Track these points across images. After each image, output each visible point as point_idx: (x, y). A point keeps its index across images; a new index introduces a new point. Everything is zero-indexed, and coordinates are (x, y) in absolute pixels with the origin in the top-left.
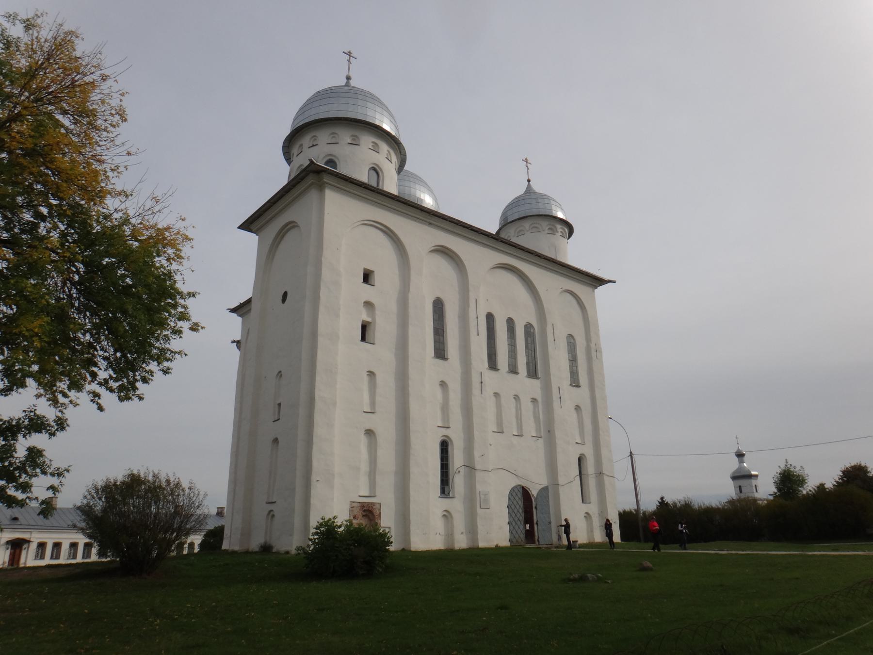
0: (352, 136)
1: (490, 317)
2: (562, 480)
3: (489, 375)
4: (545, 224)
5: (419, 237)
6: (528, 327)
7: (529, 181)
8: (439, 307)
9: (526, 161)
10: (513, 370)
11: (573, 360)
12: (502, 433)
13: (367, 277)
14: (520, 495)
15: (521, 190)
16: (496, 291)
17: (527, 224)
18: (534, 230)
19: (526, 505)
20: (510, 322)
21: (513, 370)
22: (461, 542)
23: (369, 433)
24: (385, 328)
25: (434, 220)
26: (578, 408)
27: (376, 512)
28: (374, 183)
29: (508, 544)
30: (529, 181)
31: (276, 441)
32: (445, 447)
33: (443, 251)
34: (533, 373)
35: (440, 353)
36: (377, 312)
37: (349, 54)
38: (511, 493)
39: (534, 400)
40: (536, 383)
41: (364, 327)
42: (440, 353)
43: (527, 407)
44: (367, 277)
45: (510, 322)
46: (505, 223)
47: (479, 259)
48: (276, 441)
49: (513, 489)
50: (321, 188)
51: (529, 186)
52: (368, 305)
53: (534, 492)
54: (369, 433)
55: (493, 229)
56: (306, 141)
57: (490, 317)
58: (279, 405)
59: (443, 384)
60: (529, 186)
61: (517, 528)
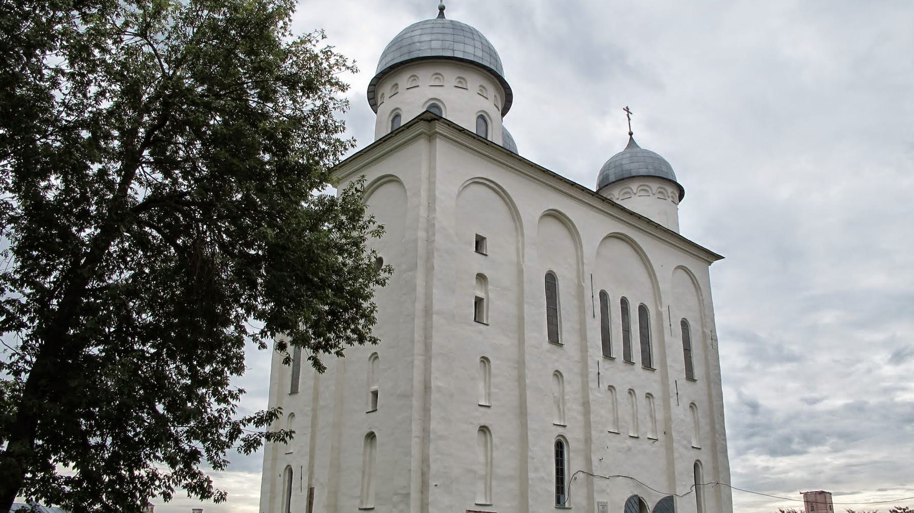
1: (603, 295)
2: (680, 491)
3: (605, 365)
4: (655, 186)
5: (533, 201)
6: (643, 310)
7: (631, 134)
8: (551, 280)
9: (627, 109)
10: (628, 359)
11: (687, 350)
13: (480, 243)
14: (637, 507)
15: (620, 146)
16: (597, 260)
17: (634, 186)
18: (643, 193)
20: (624, 302)
21: (628, 359)
23: (484, 429)
24: (499, 305)
26: (693, 405)
28: (483, 136)
30: (631, 134)
31: (371, 436)
32: (560, 447)
33: (554, 215)
34: (647, 364)
35: (554, 337)
36: (490, 287)
39: (649, 396)
41: (478, 302)
42: (554, 337)
44: (480, 243)
45: (624, 302)
46: (606, 183)
47: (593, 225)
48: (371, 436)
49: (629, 500)
50: (431, 137)
51: (631, 138)
52: (481, 277)
53: (651, 505)
56: (404, 80)
57: (603, 295)
58: (375, 394)
59: (558, 374)
60: (631, 138)
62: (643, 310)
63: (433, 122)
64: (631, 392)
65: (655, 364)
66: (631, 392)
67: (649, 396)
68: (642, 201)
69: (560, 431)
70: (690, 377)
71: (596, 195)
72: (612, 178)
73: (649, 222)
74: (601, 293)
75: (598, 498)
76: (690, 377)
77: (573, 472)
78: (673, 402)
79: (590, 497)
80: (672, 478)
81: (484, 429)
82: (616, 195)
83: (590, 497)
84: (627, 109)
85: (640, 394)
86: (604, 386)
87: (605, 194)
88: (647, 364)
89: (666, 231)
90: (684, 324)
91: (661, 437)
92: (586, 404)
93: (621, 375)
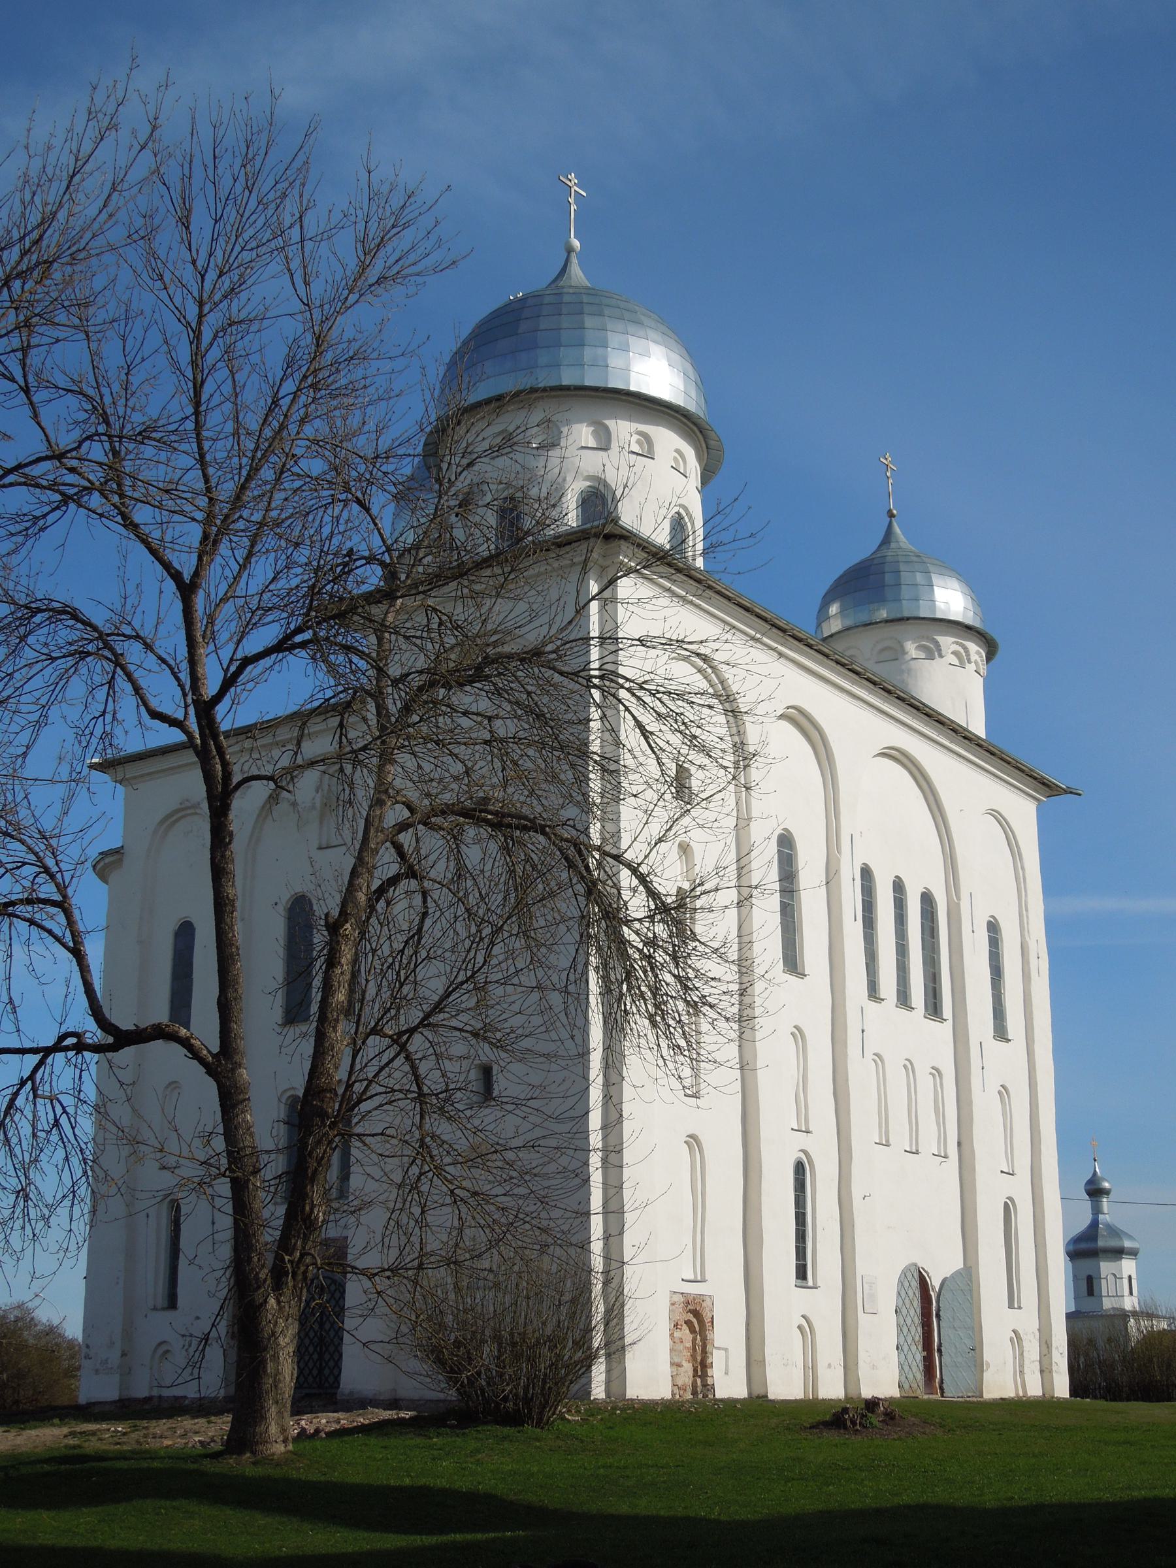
0: (678, 451)
1: (866, 873)
6: (927, 899)
10: (904, 999)
12: (917, 1153)
14: (915, 1284)
19: (932, 1310)
20: (899, 887)
21: (904, 999)
22: (832, 1389)
29: (895, 1393)
32: (800, 1168)
38: (901, 1283)
40: (943, 1031)
43: (925, 1083)
45: (899, 887)
49: (904, 1274)
53: (935, 1282)
54: (693, 1141)
57: (866, 873)
61: (910, 1357)
62: (927, 899)
63: (616, 543)
69: (802, 1141)
70: (1001, 1033)
74: (862, 869)
90: (993, 928)
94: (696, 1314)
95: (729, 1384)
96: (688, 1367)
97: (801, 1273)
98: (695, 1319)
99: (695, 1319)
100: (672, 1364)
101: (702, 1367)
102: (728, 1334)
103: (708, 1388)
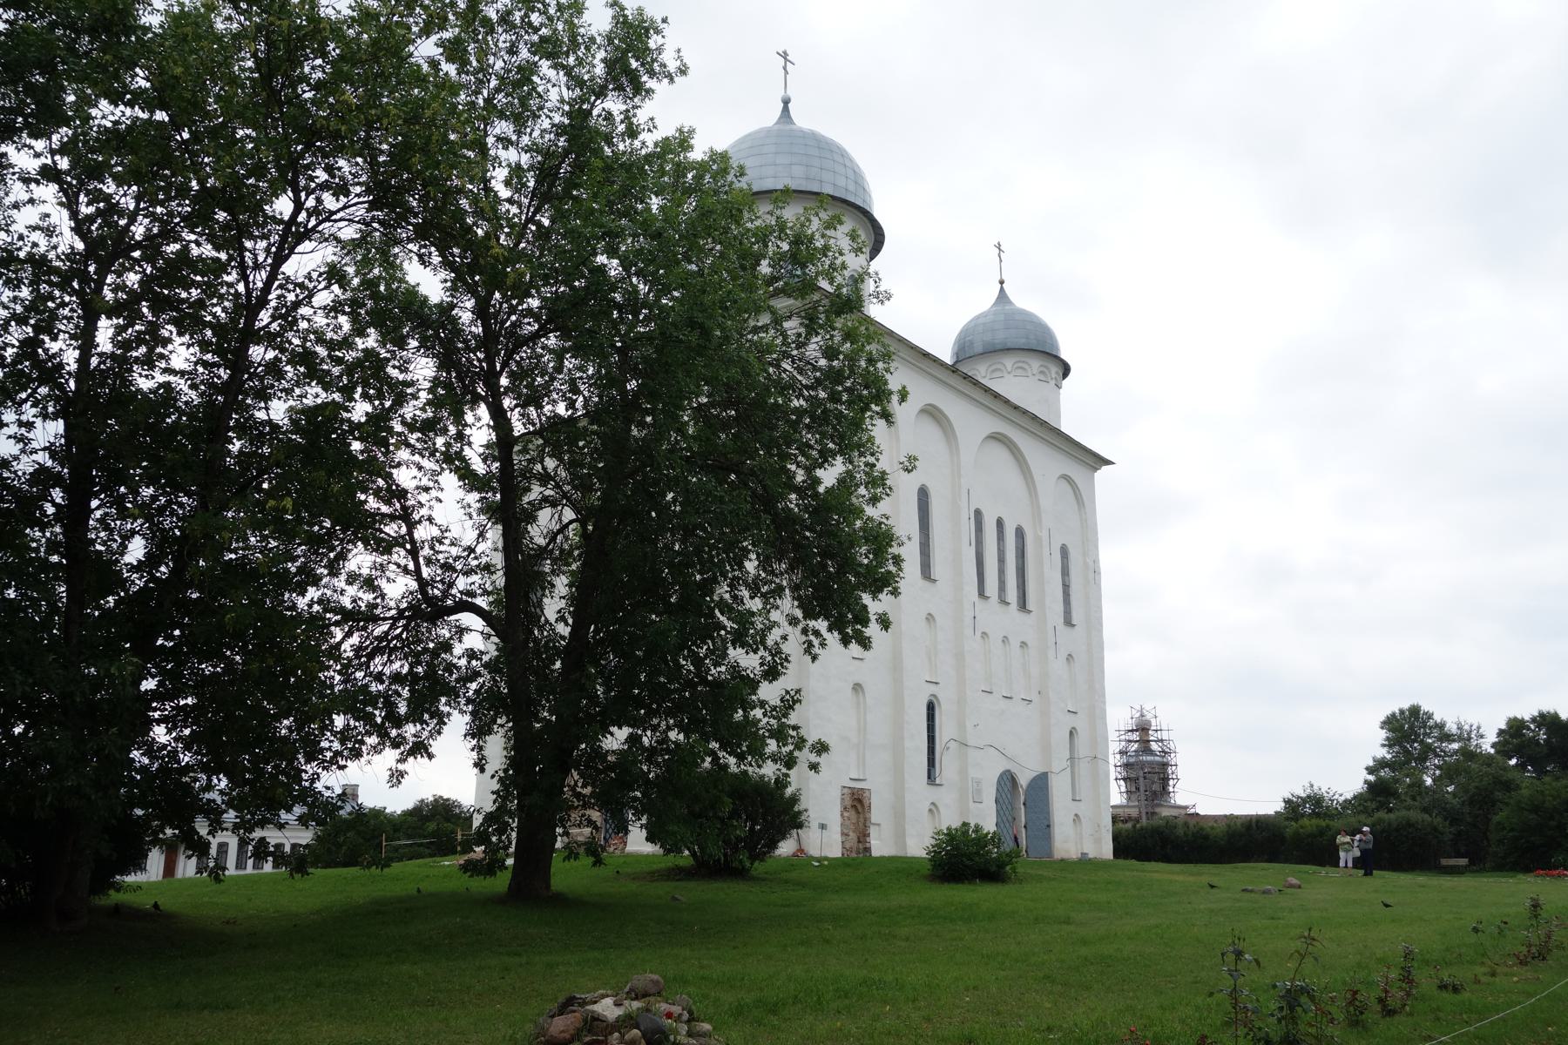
1: (978, 513)
4: (1035, 364)
6: (1020, 533)
7: (1002, 282)
9: (999, 246)
17: (1009, 362)
18: (1019, 372)
20: (1000, 523)
23: (857, 687)
25: (925, 364)
27: (866, 803)
30: (1002, 282)
32: (931, 708)
34: (1023, 605)
37: (785, 55)
39: (1024, 644)
45: (1000, 523)
49: (1001, 776)
51: (1002, 289)
53: (1023, 781)
55: (948, 359)
57: (978, 513)
59: (930, 618)
60: (1002, 289)
62: (1020, 533)
64: (1005, 640)
65: (1031, 605)
66: (1005, 640)
67: (1024, 644)
68: (1015, 383)
69: (933, 689)
70: (1068, 622)
71: (953, 369)
72: (978, 348)
73: (1034, 418)
75: (973, 773)
76: (1068, 622)
77: (945, 739)
78: (1051, 653)
79: (963, 772)
80: (1046, 749)
81: (857, 687)
82: (981, 372)
83: (963, 772)
84: (999, 246)
85: (1015, 642)
86: (978, 634)
87: (964, 368)
88: (1023, 605)
89: (1044, 424)
91: (1034, 696)
92: (960, 657)
93: (1001, 619)
94: (860, 801)
95: (880, 846)
96: (853, 836)
97: (931, 777)
98: (857, 803)
99: (857, 803)
100: (843, 834)
101: (863, 836)
102: (879, 812)
103: (868, 850)
